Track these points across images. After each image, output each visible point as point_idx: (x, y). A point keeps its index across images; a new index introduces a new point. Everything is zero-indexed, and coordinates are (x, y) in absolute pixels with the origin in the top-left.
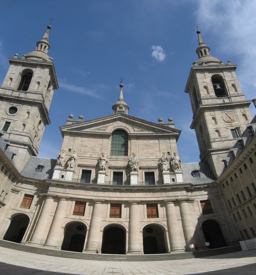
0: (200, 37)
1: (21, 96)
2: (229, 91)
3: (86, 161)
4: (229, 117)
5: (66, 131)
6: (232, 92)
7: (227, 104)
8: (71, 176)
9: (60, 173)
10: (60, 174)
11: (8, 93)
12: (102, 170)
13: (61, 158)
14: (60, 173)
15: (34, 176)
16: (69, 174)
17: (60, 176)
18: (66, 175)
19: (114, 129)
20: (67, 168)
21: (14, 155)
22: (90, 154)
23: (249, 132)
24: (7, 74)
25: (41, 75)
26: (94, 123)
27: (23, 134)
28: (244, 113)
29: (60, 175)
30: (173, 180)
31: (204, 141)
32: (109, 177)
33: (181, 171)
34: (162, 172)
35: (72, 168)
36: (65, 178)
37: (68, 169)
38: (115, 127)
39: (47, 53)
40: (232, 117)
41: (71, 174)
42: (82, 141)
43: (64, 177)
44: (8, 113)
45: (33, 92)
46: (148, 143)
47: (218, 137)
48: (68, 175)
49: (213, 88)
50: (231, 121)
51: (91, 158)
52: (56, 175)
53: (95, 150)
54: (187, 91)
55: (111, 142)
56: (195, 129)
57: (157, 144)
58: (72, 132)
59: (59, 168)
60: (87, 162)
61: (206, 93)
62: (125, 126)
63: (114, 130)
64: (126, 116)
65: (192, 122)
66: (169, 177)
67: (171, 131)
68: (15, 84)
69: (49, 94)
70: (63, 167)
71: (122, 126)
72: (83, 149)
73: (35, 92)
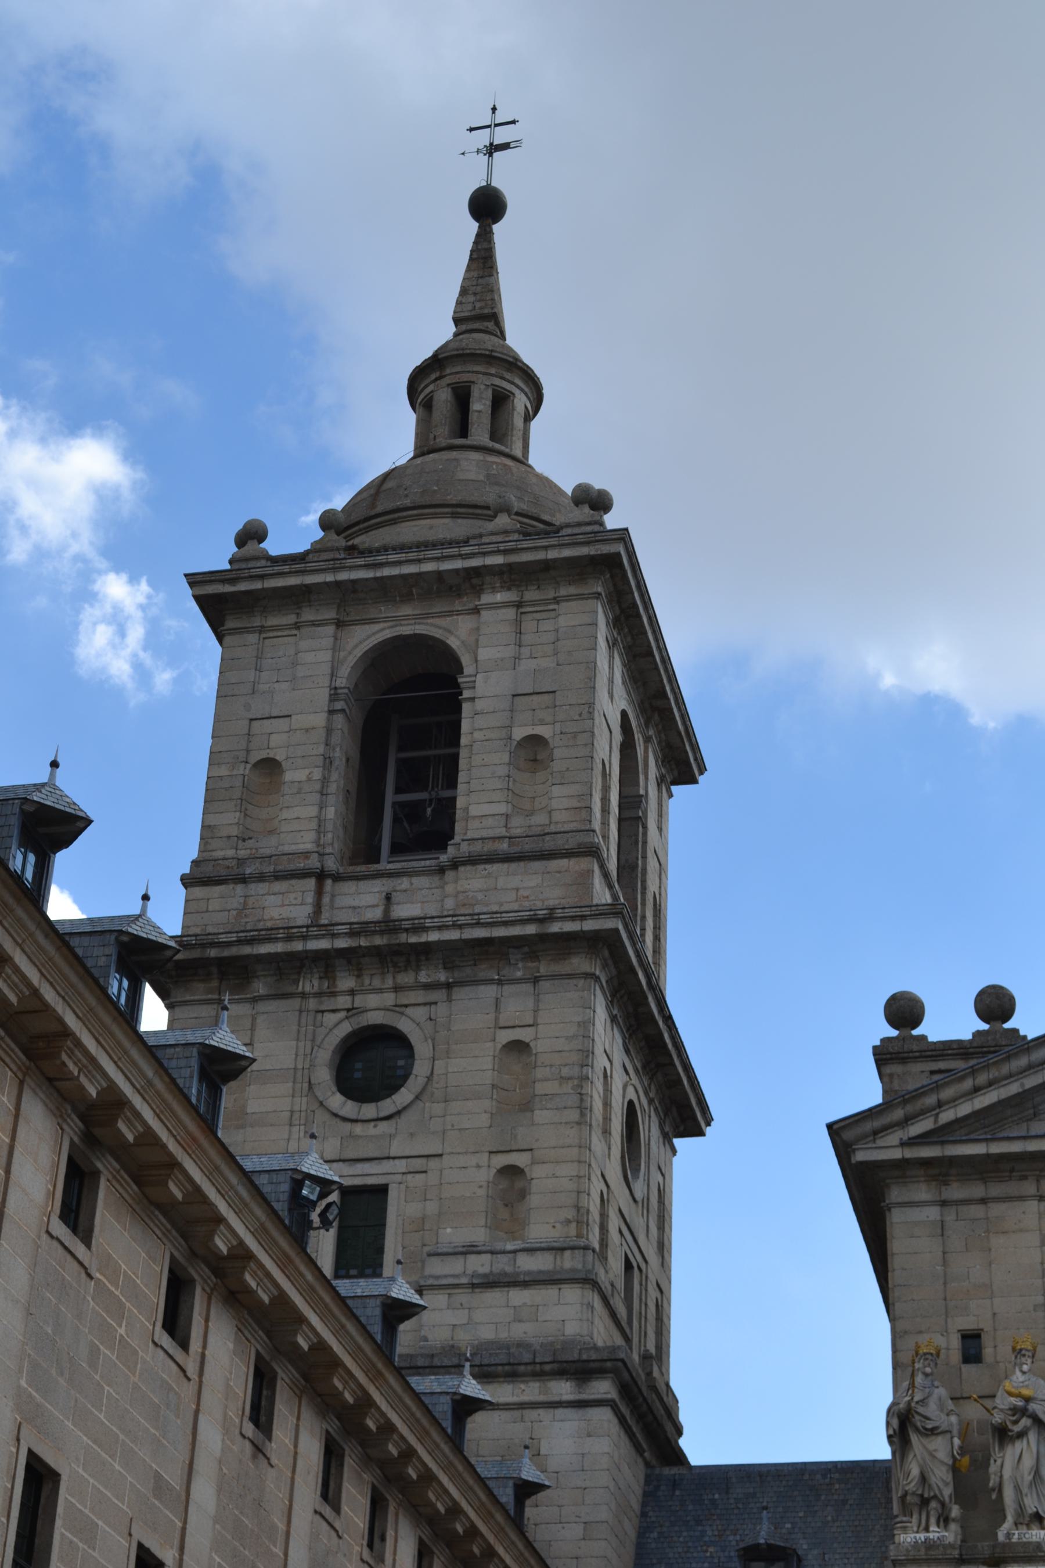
5: (897, 1154)
13: (917, 1430)
20: (1001, 1537)
37: (1009, 1535)
59: (929, 1545)
70: (953, 1526)
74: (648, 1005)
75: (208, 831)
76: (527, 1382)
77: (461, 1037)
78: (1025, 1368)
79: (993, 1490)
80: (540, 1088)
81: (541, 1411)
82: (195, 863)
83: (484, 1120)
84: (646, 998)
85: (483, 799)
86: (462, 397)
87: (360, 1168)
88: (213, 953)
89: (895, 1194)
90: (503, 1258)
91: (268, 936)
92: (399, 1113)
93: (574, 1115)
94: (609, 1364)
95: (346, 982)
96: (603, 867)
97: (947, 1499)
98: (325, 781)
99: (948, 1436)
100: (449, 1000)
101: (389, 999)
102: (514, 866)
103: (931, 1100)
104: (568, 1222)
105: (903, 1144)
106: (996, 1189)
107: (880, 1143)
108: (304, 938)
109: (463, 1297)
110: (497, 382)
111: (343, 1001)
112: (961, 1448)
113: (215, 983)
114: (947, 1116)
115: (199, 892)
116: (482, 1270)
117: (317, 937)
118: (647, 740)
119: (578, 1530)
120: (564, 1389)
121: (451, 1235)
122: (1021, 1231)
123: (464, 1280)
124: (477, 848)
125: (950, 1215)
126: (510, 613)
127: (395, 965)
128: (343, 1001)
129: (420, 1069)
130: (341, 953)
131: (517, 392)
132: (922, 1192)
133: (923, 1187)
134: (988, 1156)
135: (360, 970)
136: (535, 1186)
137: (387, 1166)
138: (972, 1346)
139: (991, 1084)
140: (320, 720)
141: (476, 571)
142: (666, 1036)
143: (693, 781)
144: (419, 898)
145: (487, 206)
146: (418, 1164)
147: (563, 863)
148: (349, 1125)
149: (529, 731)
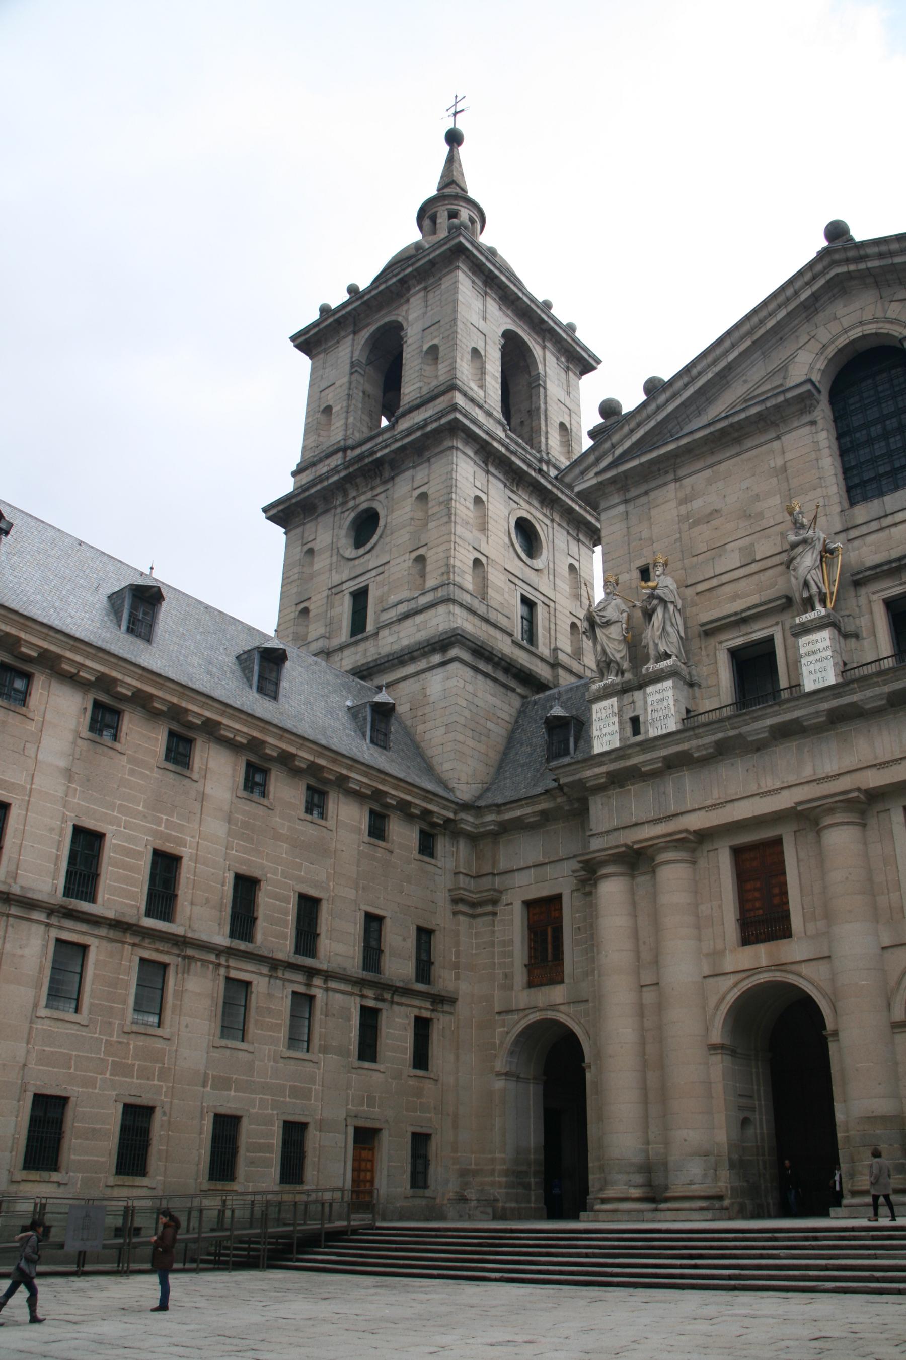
3: (735, 597)
5: (594, 481)
8: (672, 706)
9: (616, 710)
10: (620, 716)
13: (600, 626)
14: (620, 710)
16: (658, 696)
17: (622, 729)
18: (646, 709)
19: (823, 357)
20: (644, 671)
26: (710, 375)
29: (620, 723)
32: (867, 643)
35: (667, 656)
36: (647, 732)
38: (824, 347)
41: (666, 694)
42: (684, 501)
43: (642, 730)
48: (656, 706)
51: (754, 567)
53: (760, 515)
58: (624, 472)
59: (606, 687)
62: (880, 314)
63: (826, 362)
64: (862, 252)
71: (861, 323)
72: (703, 535)
74: (513, 463)
75: (304, 448)
76: (420, 661)
78: (658, 573)
79: (645, 647)
80: (430, 512)
81: (427, 674)
82: (298, 465)
83: (407, 537)
84: (510, 459)
88: (294, 501)
89: (603, 505)
90: (413, 602)
92: (373, 548)
93: (445, 519)
94: (453, 639)
95: (353, 493)
97: (618, 659)
98: (348, 406)
99: (619, 624)
100: (394, 485)
101: (369, 495)
102: (421, 410)
103: (607, 445)
104: (443, 574)
105: (597, 474)
106: (653, 484)
107: (586, 478)
108: (327, 478)
109: (395, 628)
110: (449, 207)
111: (351, 504)
112: (627, 629)
113: (302, 516)
114: (619, 451)
115: (299, 477)
116: (403, 611)
117: (332, 476)
118: (544, 347)
119: (442, 730)
120: (437, 658)
121: (393, 599)
122: (667, 502)
123: (395, 619)
125: (631, 507)
126: (422, 294)
127: (371, 478)
129: (382, 523)
130: (343, 478)
131: (459, 208)
132: (616, 499)
133: (616, 496)
134: (641, 465)
135: (357, 486)
136: (428, 561)
137: (368, 576)
138: (645, 573)
139: (639, 425)
140: (345, 380)
141: (402, 281)
142: (542, 481)
143: (593, 368)
145: (454, 138)
146: (380, 570)
148: (353, 562)
149: (430, 344)
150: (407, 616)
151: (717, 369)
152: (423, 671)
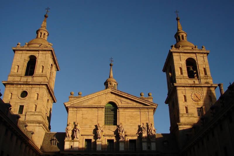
0: (179, 23)
1: (28, 81)
2: (200, 73)
4: (197, 96)
5: (69, 106)
6: (202, 74)
7: (196, 84)
11: (17, 79)
12: (99, 139)
15: (51, 150)
21: (33, 133)
22: (90, 125)
23: (211, 113)
24: (13, 62)
25: (44, 60)
27: (36, 113)
28: (210, 95)
30: (149, 148)
31: (175, 116)
33: (155, 140)
34: (141, 140)
39: (46, 40)
40: (199, 97)
44: (20, 97)
45: (38, 76)
46: (132, 114)
47: (185, 113)
49: (186, 70)
50: (198, 100)
52: (67, 146)
53: (93, 121)
54: (164, 70)
55: (104, 113)
56: (168, 104)
57: (138, 115)
60: (87, 133)
61: (180, 74)
65: (167, 98)
66: (146, 145)
67: (150, 104)
68: (23, 71)
69: (52, 76)
73: (41, 76)
77: (33, 93)
85: (38, 70)
86: (41, 33)
87: (22, 104)
89: (69, 109)
91: (15, 82)
96: (47, 78)
103: (73, 102)
109: (29, 116)
120: (38, 125)
124: (36, 75)
128: (22, 88)
129: (28, 95)
140: (23, 62)
144: (29, 79)
147: (43, 77)
150: (32, 115)
151: (93, 97)
152: (35, 126)
